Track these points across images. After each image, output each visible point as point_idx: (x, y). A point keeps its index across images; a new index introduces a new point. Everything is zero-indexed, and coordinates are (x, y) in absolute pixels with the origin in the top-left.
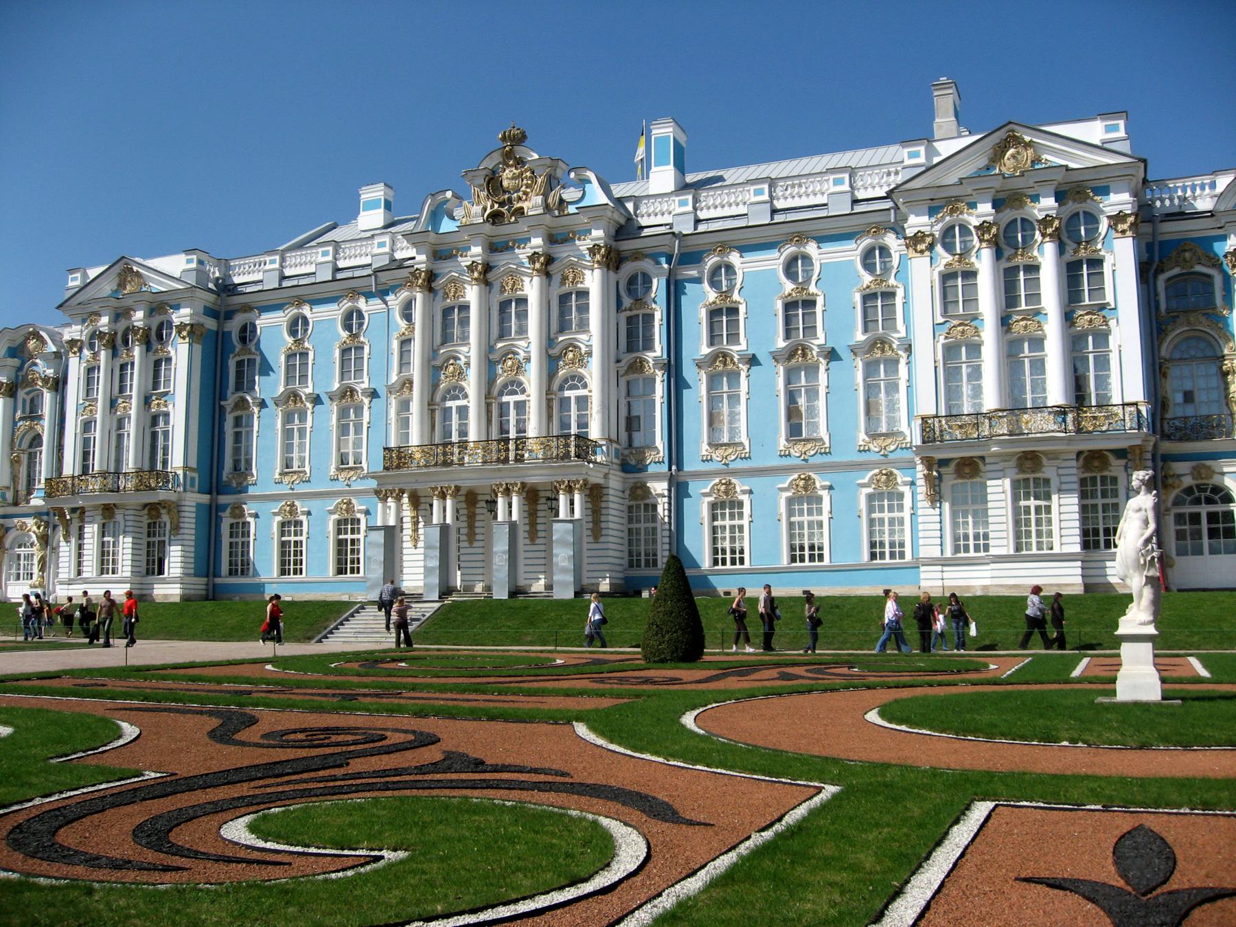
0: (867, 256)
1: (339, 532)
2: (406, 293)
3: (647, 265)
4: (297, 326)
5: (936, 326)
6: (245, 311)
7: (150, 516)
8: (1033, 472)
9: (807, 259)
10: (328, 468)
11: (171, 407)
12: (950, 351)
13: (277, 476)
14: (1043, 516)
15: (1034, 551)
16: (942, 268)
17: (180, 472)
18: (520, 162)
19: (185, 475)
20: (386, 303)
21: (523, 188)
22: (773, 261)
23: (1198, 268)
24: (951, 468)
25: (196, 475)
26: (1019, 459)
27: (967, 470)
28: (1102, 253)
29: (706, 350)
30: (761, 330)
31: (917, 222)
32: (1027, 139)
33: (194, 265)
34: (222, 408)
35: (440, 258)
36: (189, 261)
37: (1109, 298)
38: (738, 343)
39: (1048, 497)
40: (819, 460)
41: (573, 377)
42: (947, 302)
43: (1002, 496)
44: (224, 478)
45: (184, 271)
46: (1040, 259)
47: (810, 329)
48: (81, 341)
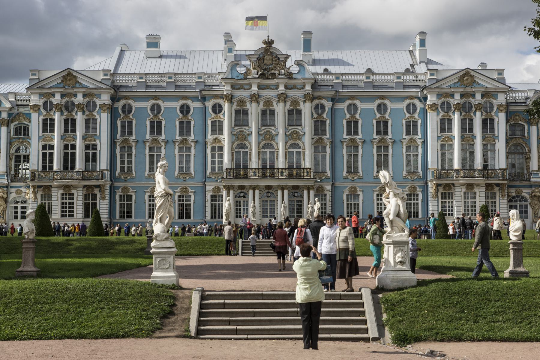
3: (324, 102)
4: (156, 109)
5: (438, 138)
6: (127, 99)
9: (385, 105)
11: (98, 142)
12: (442, 146)
20: (204, 104)
23: (520, 122)
27: (447, 188)
30: (367, 130)
34: (115, 142)
35: (234, 89)
38: (358, 134)
44: (117, 175)
45: (103, 79)
46: (474, 117)
48: (40, 105)
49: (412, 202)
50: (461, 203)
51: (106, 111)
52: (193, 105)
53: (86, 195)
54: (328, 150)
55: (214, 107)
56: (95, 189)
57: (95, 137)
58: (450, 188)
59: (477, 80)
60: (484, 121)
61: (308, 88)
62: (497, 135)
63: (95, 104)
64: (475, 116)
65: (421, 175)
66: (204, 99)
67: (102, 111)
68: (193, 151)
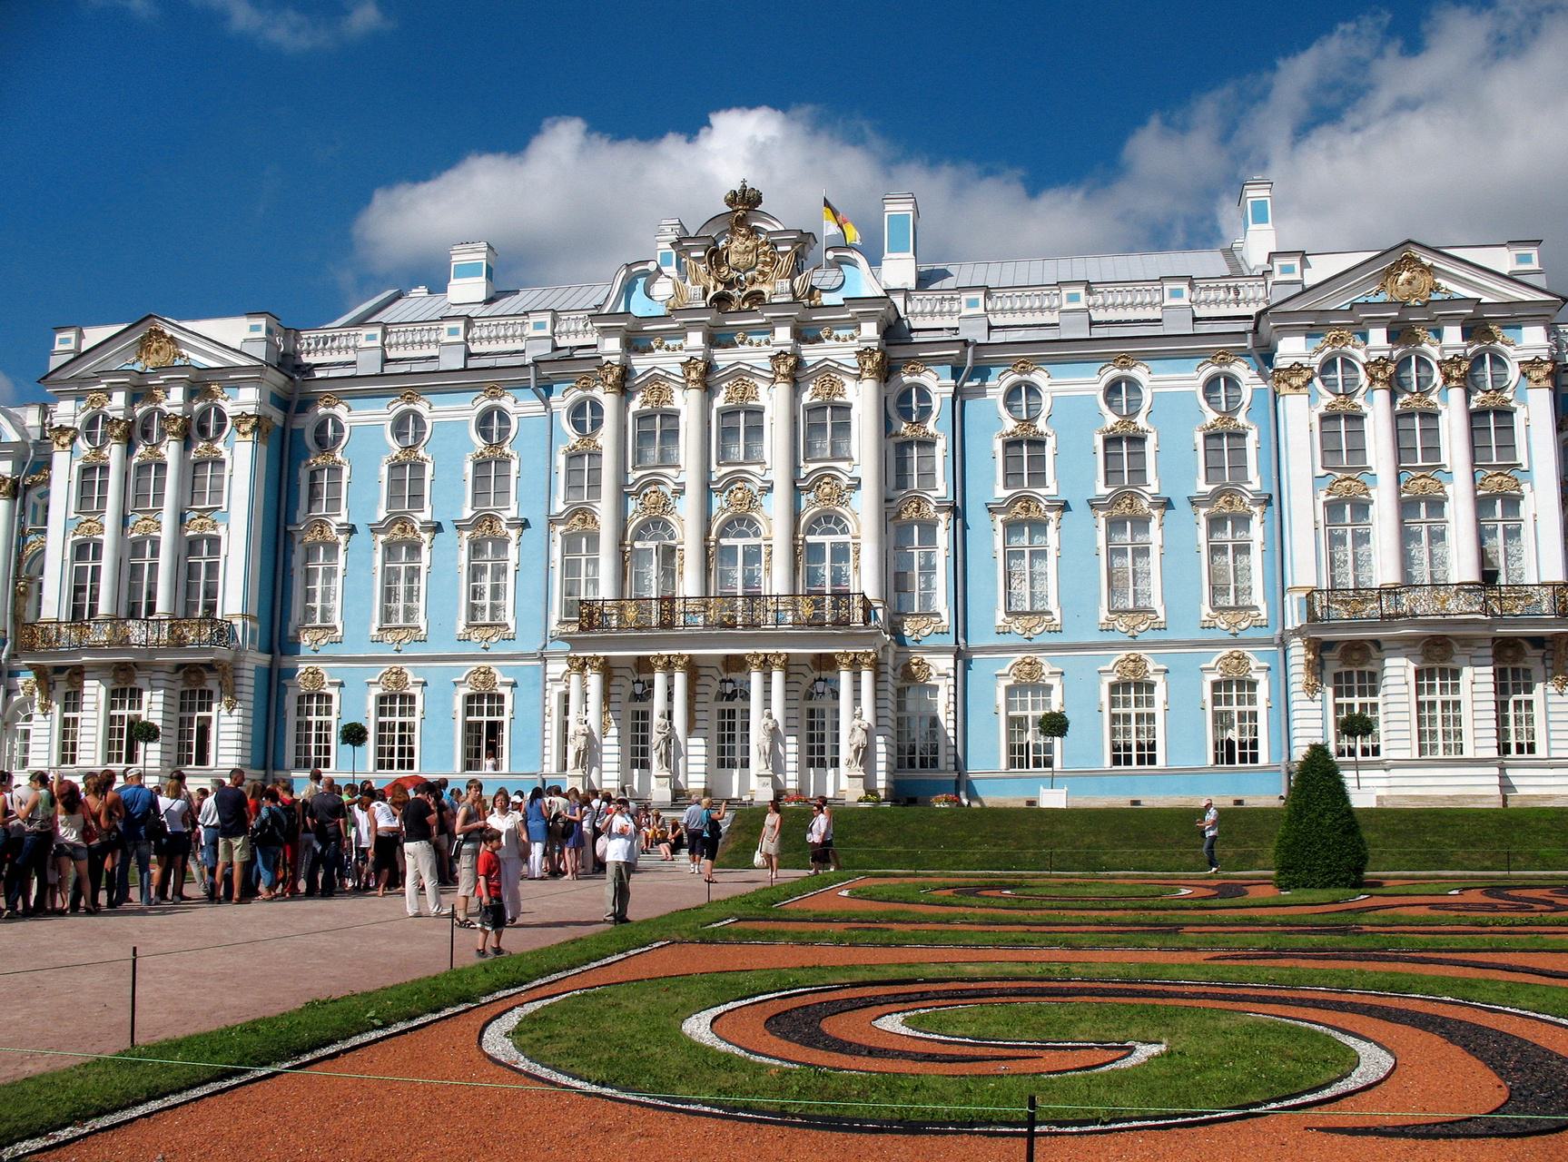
0: (1211, 385)
1: (469, 712)
2: (579, 392)
7: (186, 679)
8: (1442, 661)
10: (454, 624)
12: (1333, 509)
13: (374, 632)
14: (1426, 713)
15: (1440, 755)
16: (1322, 410)
17: (238, 622)
18: (755, 231)
19: (244, 625)
21: (759, 267)
22: (1089, 383)
24: (1336, 654)
25: (256, 626)
26: (1427, 644)
28: (1513, 404)
29: (1001, 493)
30: (1072, 469)
31: (1291, 349)
32: (1427, 262)
33: (262, 334)
36: (254, 328)
37: (1521, 457)
38: (1043, 484)
39: (1529, 690)
40: (1151, 636)
41: (828, 519)
42: (1329, 450)
43: (1405, 689)
47: (1139, 473)
49: (1235, 708)
50: (1405, 707)
51: (250, 437)
52: (520, 406)
53: (183, 694)
54: (943, 537)
55: (577, 411)
56: (207, 675)
57: (214, 516)
58: (1366, 657)
59: (1444, 283)
60: (1476, 418)
61: (870, 330)
62: (1525, 467)
63: (221, 416)
64: (1445, 401)
65: (1264, 616)
66: (545, 389)
67: (239, 437)
68: (512, 552)
